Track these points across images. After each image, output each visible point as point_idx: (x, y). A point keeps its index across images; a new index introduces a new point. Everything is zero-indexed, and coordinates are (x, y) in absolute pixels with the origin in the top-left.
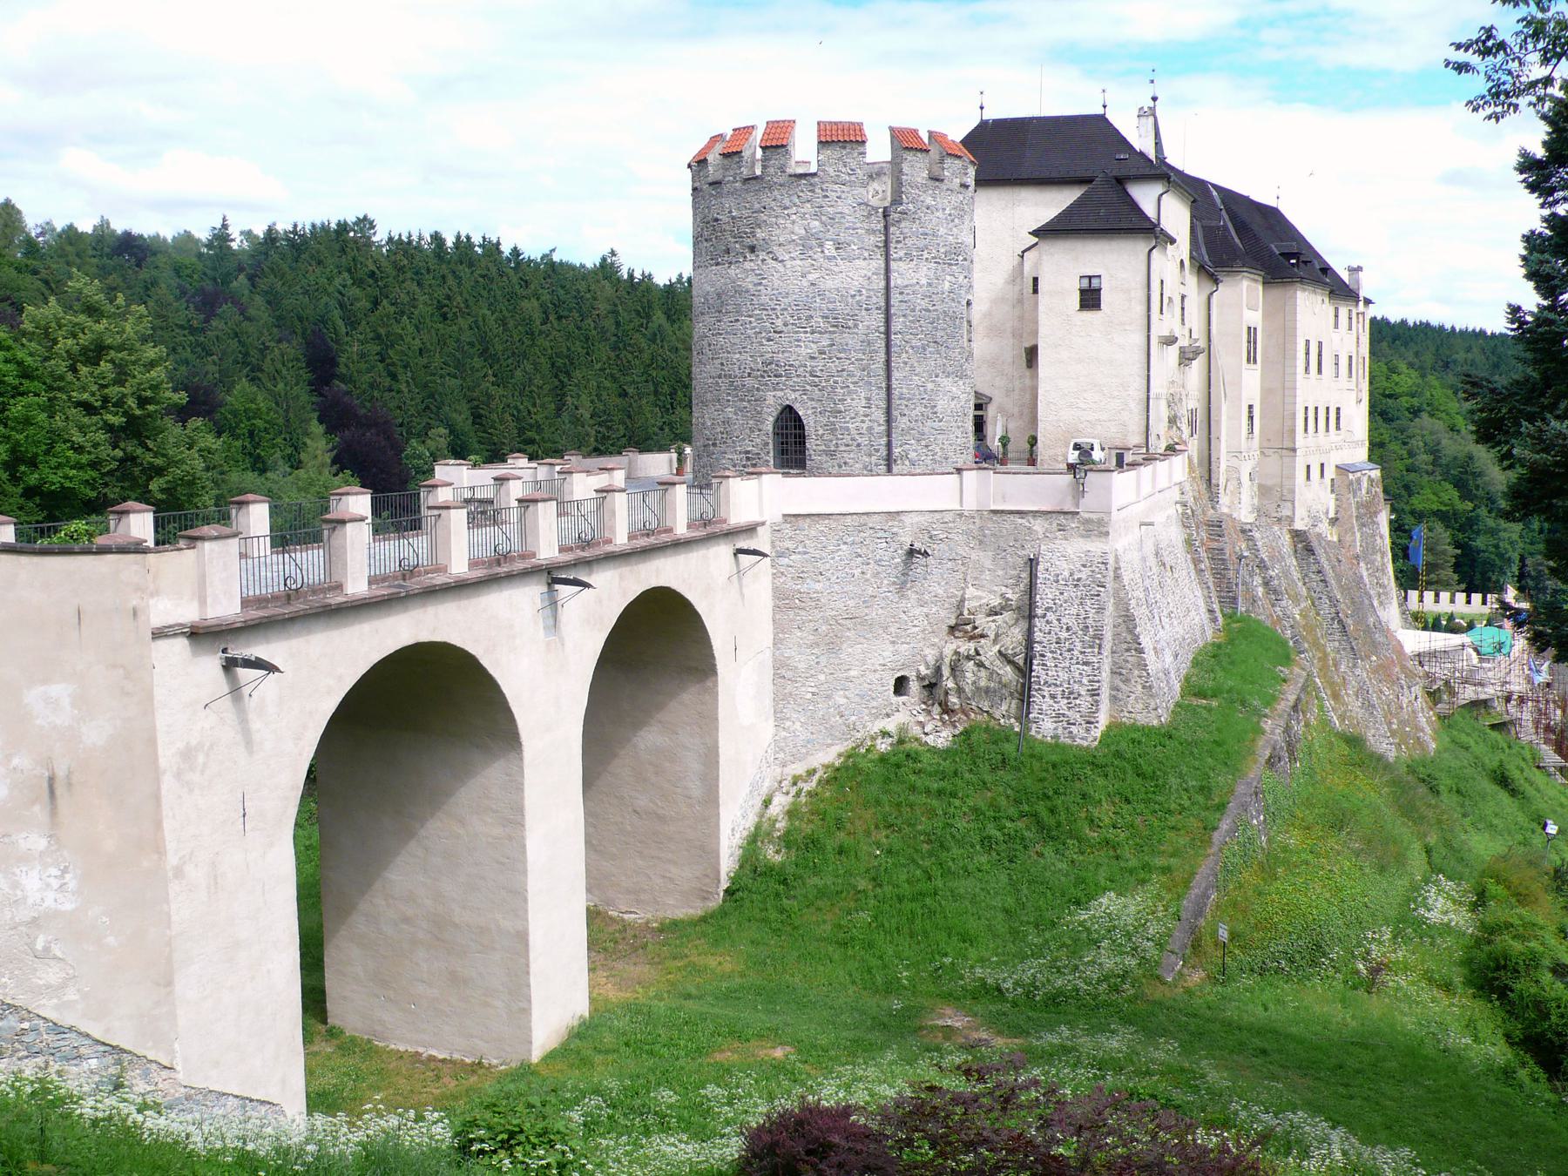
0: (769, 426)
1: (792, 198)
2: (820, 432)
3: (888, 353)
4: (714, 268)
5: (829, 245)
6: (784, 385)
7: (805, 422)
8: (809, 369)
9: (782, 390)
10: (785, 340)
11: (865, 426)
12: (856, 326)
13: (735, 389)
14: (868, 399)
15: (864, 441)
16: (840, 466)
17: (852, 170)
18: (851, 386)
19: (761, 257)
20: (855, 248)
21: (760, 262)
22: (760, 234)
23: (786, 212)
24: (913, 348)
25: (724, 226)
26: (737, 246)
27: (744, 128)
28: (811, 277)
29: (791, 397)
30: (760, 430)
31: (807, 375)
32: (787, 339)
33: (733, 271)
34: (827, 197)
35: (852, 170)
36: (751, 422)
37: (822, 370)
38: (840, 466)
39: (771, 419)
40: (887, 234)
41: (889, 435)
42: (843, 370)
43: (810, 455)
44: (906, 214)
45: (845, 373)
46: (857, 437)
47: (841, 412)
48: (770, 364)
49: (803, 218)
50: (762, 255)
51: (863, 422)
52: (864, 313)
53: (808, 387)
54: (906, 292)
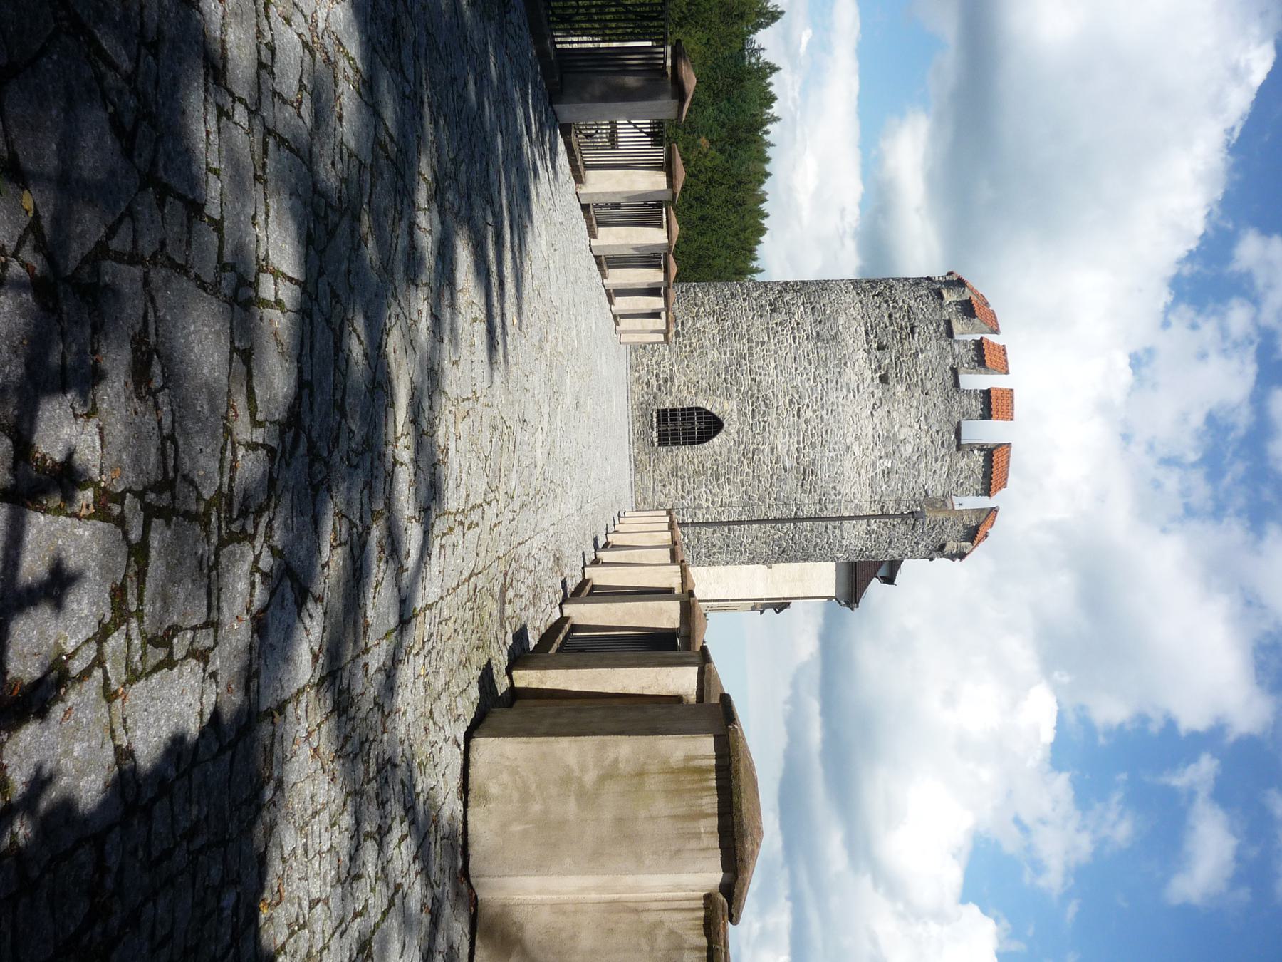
0: (701, 403)
1: (937, 425)
2: (696, 460)
3: (776, 520)
4: (863, 329)
5: (888, 463)
6: (744, 421)
7: (706, 444)
8: (762, 448)
9: (739, 419)
10: (792, 420)
11: (703, 502)
12: (803, 491)
13: (738, 362)
14: (730, 504)
15: (687, 502)
16: (661, 481)
17: (962, 483)
18: (744, 489)
19: (876, 391)
20: (883, 488)
21: (871, 389)
22: (900, 389)
23: (922, 418)
24: (780, 537)
25: (907, 343)
26: (887, 361)
27: (1006, 361)
28: (856, 448)
29: (731, 428)
30: (696, 394)
31: (755, 446)
32: (791, 423)
33: (861, 355)
34: (936, 461)
35: (962, 483)
36: (704, 384)
37: (759, 460)
38: (661, 481)
39: (708, 408)
40: (894, 516)
41: (693, 523)
42: (760, 481)
43: (672, 451)
44: (913, 529)
45: (756, 484)
46: (692, 496)
47: (717, 480)
48: (765, 403)
49: (916, 436)
50: (878, 393)
51: (707, 500)
52: (817, 498)
53: (742, 446)
54: (836, 531)
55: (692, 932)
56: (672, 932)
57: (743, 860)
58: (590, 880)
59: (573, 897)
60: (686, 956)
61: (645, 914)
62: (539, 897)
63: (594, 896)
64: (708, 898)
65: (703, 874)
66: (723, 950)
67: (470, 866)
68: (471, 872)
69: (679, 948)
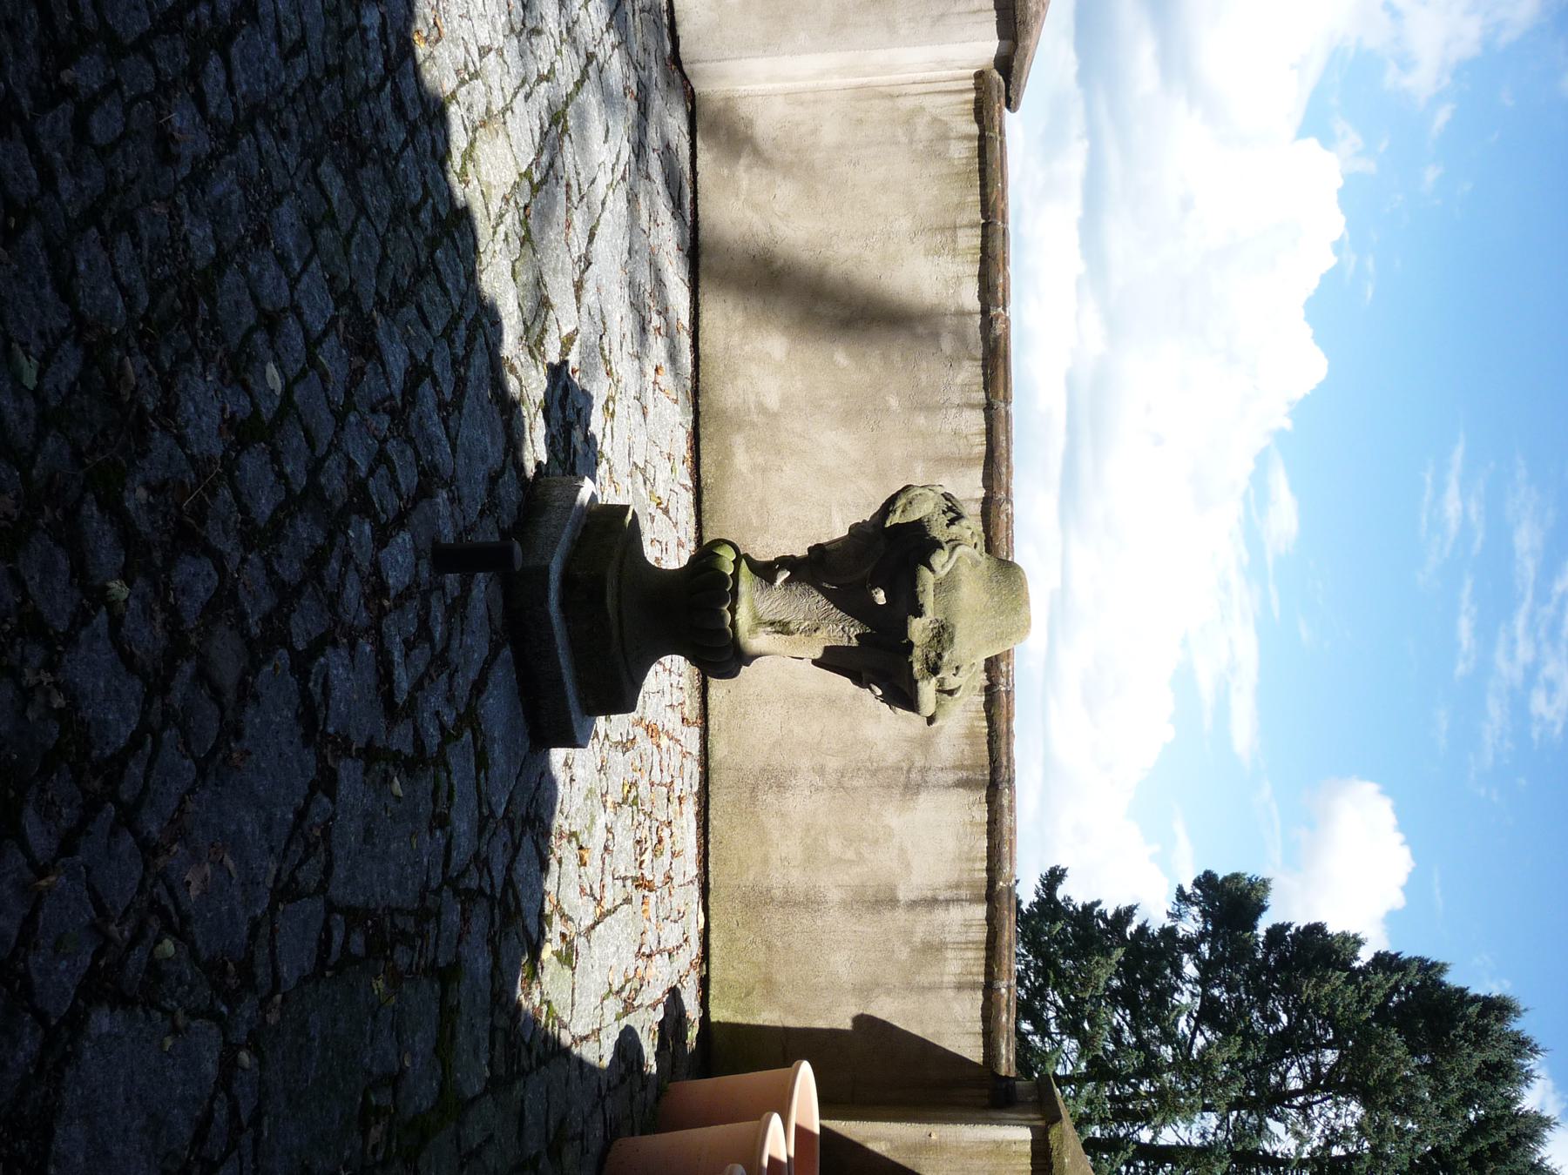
55: (959, 118)
56: (935, 120)
57: (1024, 23)
58: (831, 59)
59: (812, 84)
60: (952, 146)
61: (901, 100)
62: (770, 86)
63: (836, 81)
64: (980, 76)
65: (975, 43)
66: (999, 138)
67: (680, 50)
68: (682, 57)
69: (944, 137)
